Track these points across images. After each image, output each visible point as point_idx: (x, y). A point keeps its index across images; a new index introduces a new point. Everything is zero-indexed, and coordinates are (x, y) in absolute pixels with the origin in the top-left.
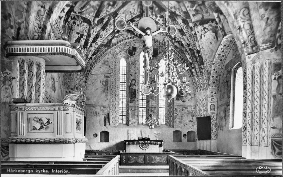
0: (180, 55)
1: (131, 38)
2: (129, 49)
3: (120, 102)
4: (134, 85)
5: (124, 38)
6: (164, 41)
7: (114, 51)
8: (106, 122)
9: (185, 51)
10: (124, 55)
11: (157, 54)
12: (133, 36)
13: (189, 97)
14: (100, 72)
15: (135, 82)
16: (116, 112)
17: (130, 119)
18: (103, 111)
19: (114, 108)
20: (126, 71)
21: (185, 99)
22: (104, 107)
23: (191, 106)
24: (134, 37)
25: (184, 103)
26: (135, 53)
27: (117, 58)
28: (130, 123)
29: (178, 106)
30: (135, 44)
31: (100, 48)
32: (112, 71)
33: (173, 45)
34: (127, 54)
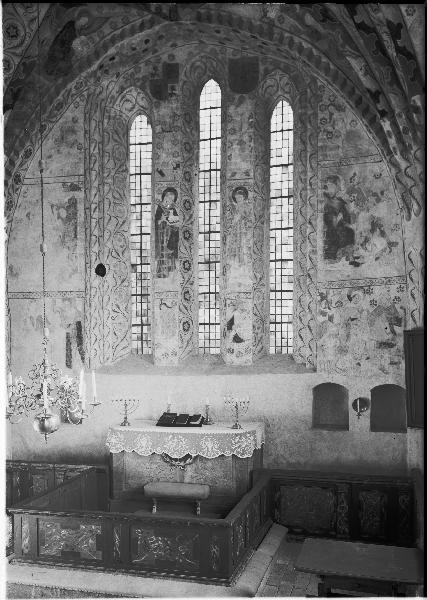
0: (332, 67)
1: (142, 27)
2: (153, 75)
4: (172, 211)
5: (118, 32)
9: (341, 41)
10: (142, 103)
12: (150, 16)
13: (379, 243)
14: (51, 172)
15: (175, 200)
21: (361, 251)
23: (388, 281)
24: (152, 23)
25: (358, 269)
26: (173, 88)
31: (18, 81)
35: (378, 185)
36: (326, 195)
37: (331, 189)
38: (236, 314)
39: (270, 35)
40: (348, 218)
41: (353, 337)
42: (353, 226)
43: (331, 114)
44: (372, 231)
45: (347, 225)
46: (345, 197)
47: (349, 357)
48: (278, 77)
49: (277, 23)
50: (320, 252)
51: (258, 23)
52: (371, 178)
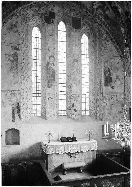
0: (110, 28)
2: (45, 14)
3: (33, 86)
4: (53, 64)
6: (92, 7)
7: (25, 14)
8: (15, 115)
10: (38, 22)
11: (81, 25)
13: (118, 83)
15: (54, 60)
16: (29, 100)
17: (48, 110)
18: (10, 99)
19: (26, 94)
20: (40, 45)
22: (11, 94)
23: (121, 93)
26: (53, 21)
27: (29, 24)
28: (48, 116)
29: (106, 93)
30: (54, 8)
32: (22, 42)
33: (102, 13)
34: (43, 20)
35: (118, 66)
36: (104, 66)
37: (106, 65)
38: (75, 102)
39: (93, 13)
40: (110, 74)
41: (112, 110)
42: (112, 77)
43: (105, 42)
44: (117, 79)
45: (110, 76)
46: (110, 68)
47: (112, 116)
48: (86, 27)
49: (95, 10)
50: (103, 84)
51: (89, 8)
52: (116, 63)
